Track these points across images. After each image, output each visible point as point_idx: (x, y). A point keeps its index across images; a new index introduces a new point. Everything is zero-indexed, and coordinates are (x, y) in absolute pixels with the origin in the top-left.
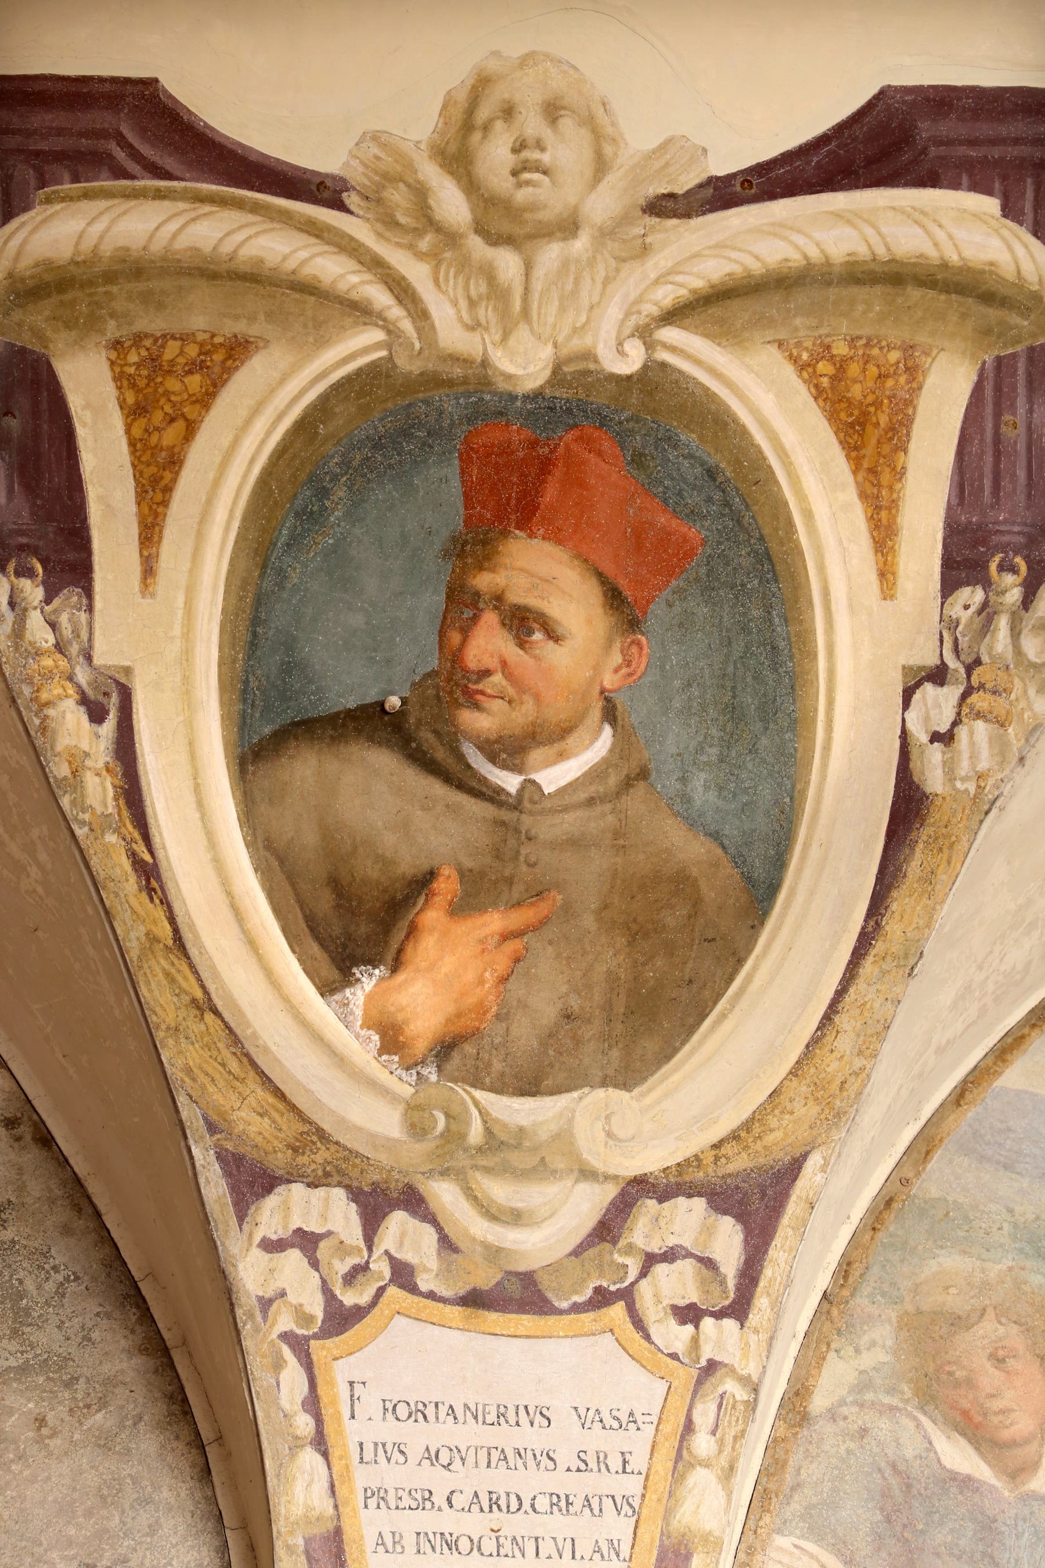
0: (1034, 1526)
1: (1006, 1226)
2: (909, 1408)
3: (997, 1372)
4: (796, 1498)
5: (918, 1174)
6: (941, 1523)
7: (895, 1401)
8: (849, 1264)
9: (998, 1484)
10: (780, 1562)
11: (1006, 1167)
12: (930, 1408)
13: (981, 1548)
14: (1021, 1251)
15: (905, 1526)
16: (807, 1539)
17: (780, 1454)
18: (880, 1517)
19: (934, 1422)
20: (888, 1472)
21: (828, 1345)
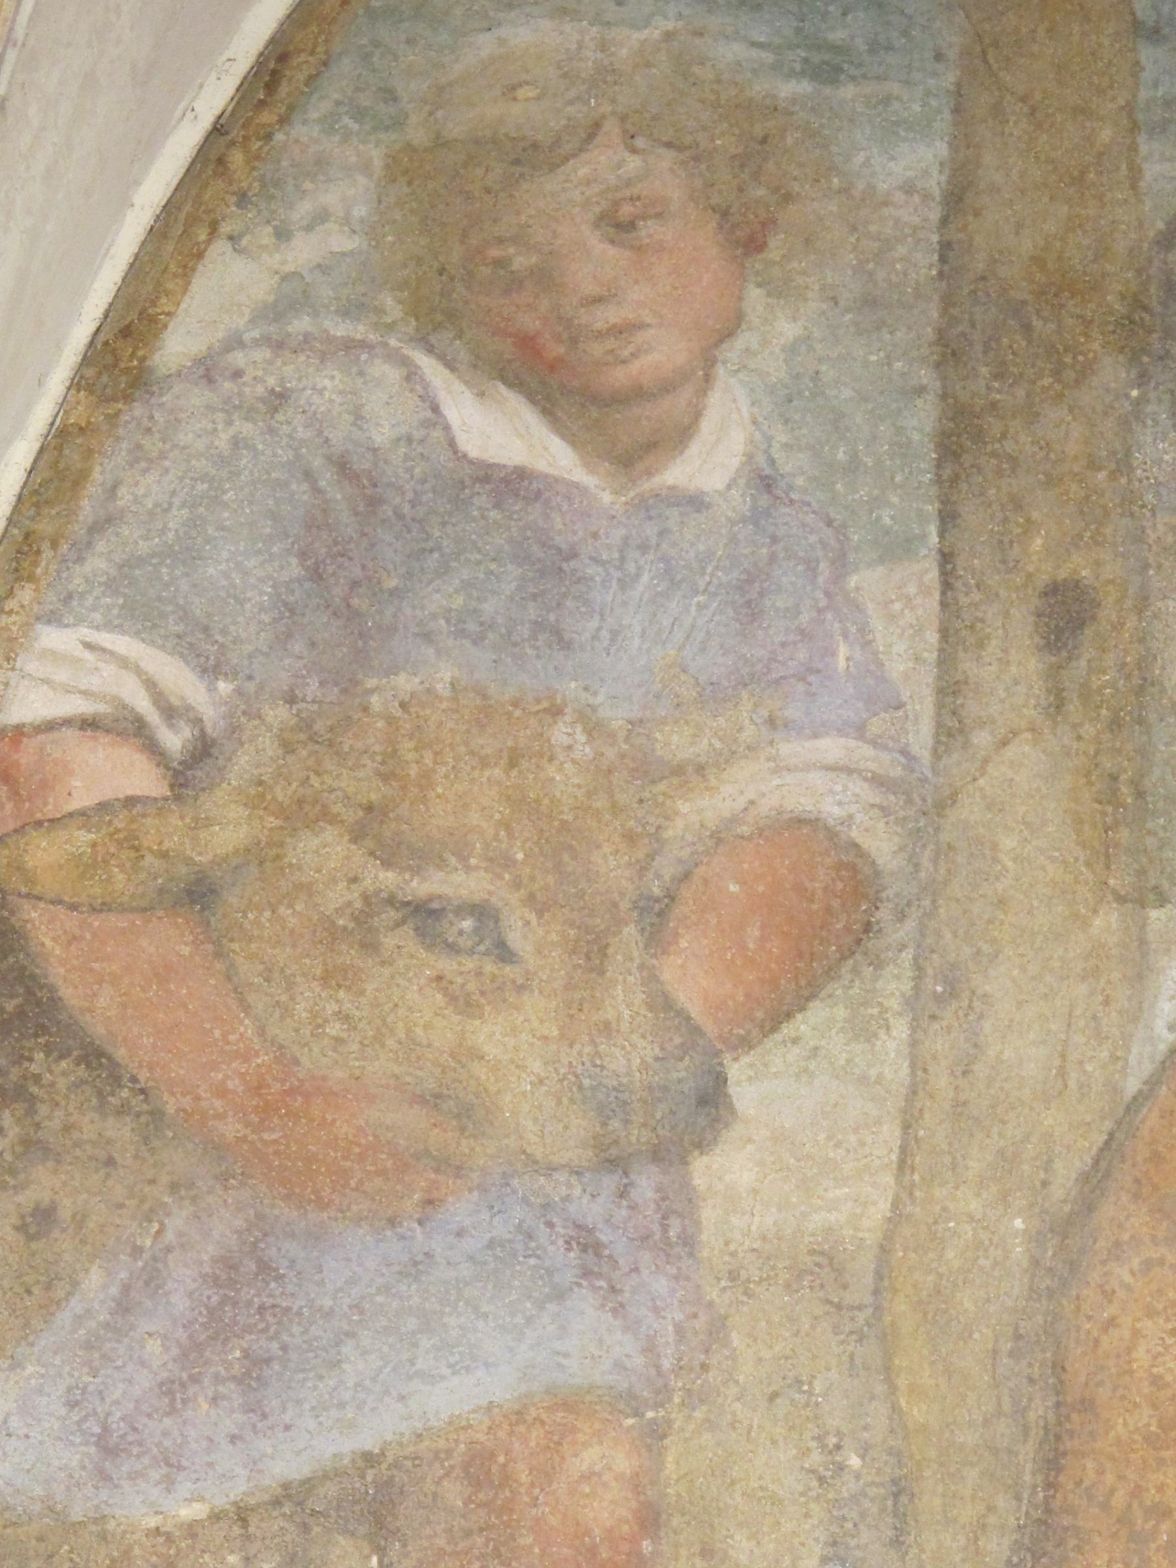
0: (665, 559)
2: (393, 342)
3: (612, 251)
4: (100, 546)
6: (444, 571)
7: (360, 330)
8: (283, 58)
9: (589, 481)
10: (46, 681)
12: (440, 339)
13: (532, 611)
16: (119, 629)
19: (450, 365)
20: (326, 478)
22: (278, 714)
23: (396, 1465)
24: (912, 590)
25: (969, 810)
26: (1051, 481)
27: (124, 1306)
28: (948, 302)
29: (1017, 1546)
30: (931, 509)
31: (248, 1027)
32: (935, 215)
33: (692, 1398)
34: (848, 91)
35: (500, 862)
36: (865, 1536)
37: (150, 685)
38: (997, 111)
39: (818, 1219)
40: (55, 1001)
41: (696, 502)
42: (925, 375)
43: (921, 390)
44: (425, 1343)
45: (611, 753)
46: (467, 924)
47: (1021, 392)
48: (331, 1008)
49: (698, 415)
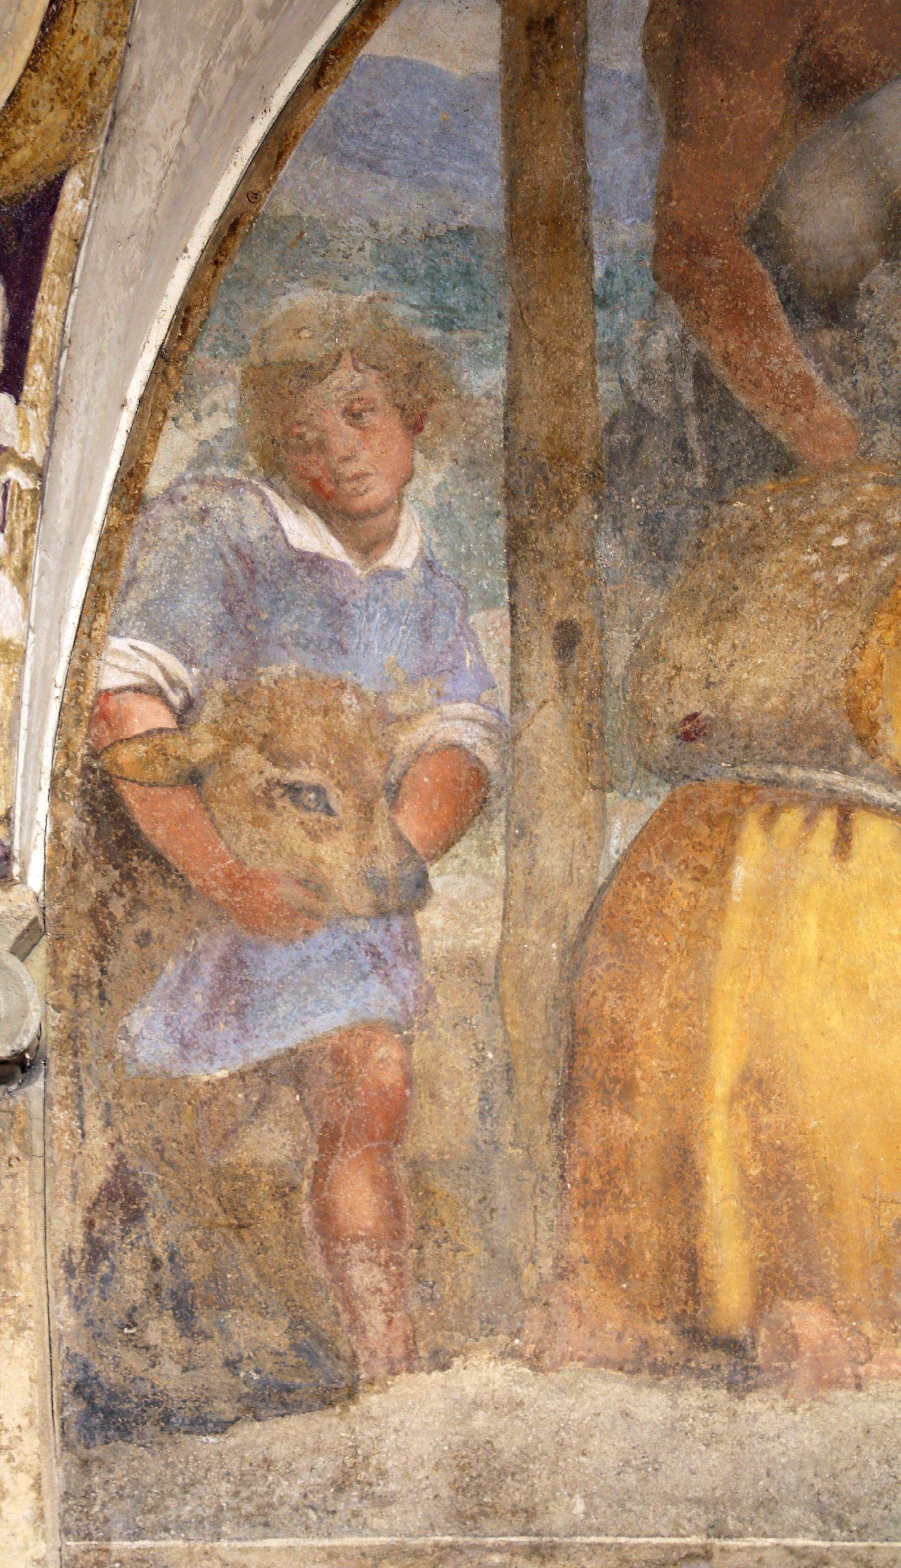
0: (386, 605)
1: (368, 245)
2: (254, 482)
3: (352, 430)
4: (132, 594)
5: (269, 185)
6: (287, 611)
8: (188, 310)
9: (349, 562)
10: (116, 666)
11: (371, 166)
13: (329, 634)
14: (384, 276)
15: (248, 617)
17: (114, 545)
18: (222, 609)
19: (282, 495)
20: (230, 558)
21: (165, 413)
22: (220, 686)
23: (303, 1054)
24: (498, 624)
25: (526, 742)
26: (559, 566)
27: (184, 979)
28: (509, 463)
29: (558, 1095)
30: (505, 580)
31: (222, 846)
32: (501, 412)
33: (421, 1028)
34: (457, 336)
35: (324, 765)
36: (496, 1089)
37: (163, 669)
38: (528, 349)
39: (470, 943)
40: (139, 831)
41: (398, 575)
42: (499, 505)
43: (498, 514)
44: (311, 998)
45: (369, 710)
46: (312, 796)
47: (544, 516)
48: (257, 837)
49: (397, 526)
